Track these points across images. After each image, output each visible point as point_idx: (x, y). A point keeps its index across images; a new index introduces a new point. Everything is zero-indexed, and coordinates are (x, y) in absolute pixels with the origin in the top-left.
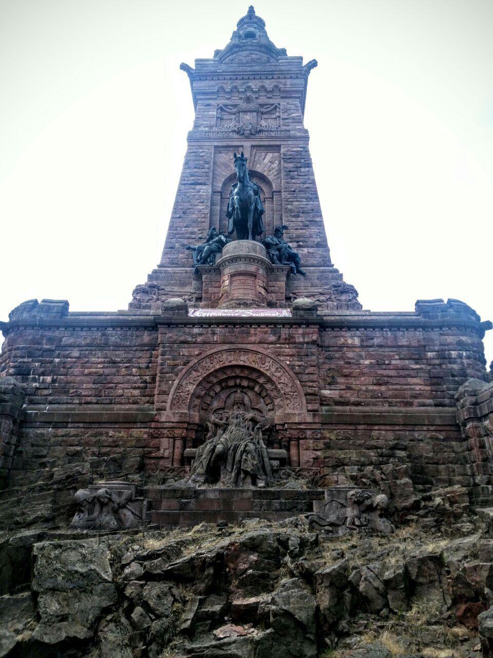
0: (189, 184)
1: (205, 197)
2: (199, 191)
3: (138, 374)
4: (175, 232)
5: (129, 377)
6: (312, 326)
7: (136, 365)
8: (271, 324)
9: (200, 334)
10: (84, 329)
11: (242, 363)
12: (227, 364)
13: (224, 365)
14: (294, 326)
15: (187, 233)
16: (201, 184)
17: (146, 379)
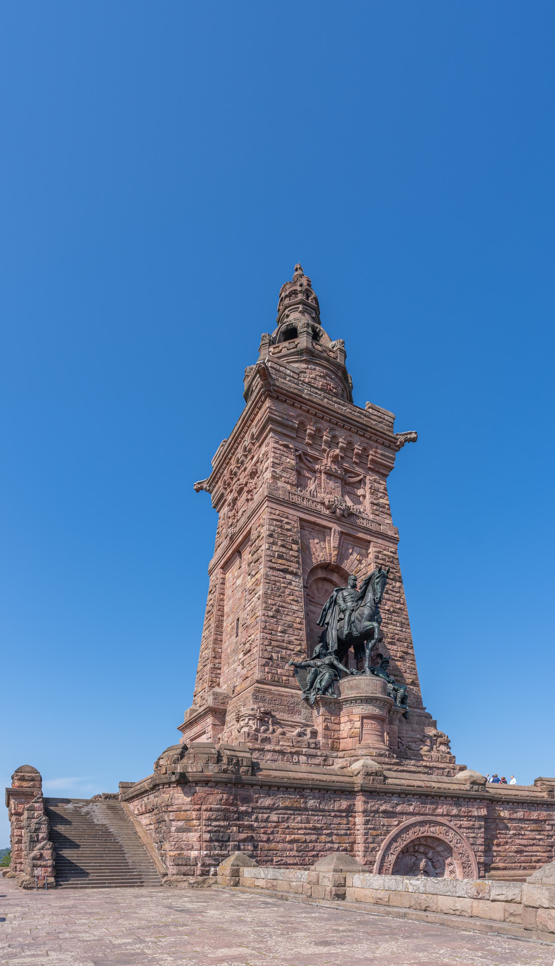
0: (278, 570)
1: (297, 593)
2: (290, 584)
3: (337, 841)
4: (269, 636)
5: (329, 845)
6: (485, 801)
7: (335, 832)
8: (456, 797)
9: (398, 804)
10: (281, 789)
11: (432, 835)
12: (420, 835)
13: (418, 836)
14: (472, 800)
15: (283, 641)
16: (291, 573)
17: (347, 847)
